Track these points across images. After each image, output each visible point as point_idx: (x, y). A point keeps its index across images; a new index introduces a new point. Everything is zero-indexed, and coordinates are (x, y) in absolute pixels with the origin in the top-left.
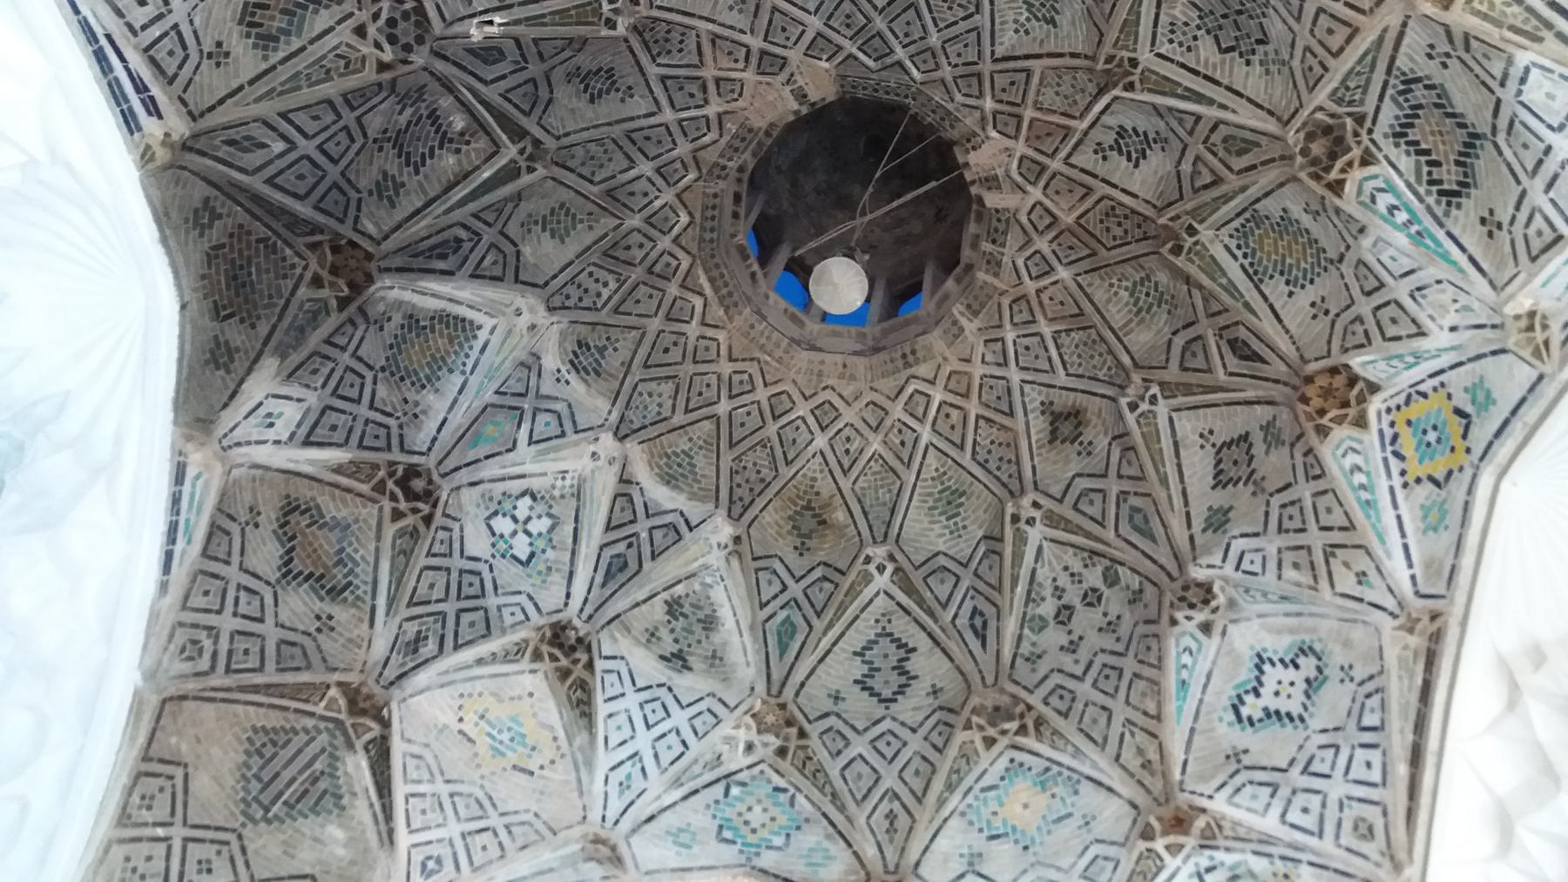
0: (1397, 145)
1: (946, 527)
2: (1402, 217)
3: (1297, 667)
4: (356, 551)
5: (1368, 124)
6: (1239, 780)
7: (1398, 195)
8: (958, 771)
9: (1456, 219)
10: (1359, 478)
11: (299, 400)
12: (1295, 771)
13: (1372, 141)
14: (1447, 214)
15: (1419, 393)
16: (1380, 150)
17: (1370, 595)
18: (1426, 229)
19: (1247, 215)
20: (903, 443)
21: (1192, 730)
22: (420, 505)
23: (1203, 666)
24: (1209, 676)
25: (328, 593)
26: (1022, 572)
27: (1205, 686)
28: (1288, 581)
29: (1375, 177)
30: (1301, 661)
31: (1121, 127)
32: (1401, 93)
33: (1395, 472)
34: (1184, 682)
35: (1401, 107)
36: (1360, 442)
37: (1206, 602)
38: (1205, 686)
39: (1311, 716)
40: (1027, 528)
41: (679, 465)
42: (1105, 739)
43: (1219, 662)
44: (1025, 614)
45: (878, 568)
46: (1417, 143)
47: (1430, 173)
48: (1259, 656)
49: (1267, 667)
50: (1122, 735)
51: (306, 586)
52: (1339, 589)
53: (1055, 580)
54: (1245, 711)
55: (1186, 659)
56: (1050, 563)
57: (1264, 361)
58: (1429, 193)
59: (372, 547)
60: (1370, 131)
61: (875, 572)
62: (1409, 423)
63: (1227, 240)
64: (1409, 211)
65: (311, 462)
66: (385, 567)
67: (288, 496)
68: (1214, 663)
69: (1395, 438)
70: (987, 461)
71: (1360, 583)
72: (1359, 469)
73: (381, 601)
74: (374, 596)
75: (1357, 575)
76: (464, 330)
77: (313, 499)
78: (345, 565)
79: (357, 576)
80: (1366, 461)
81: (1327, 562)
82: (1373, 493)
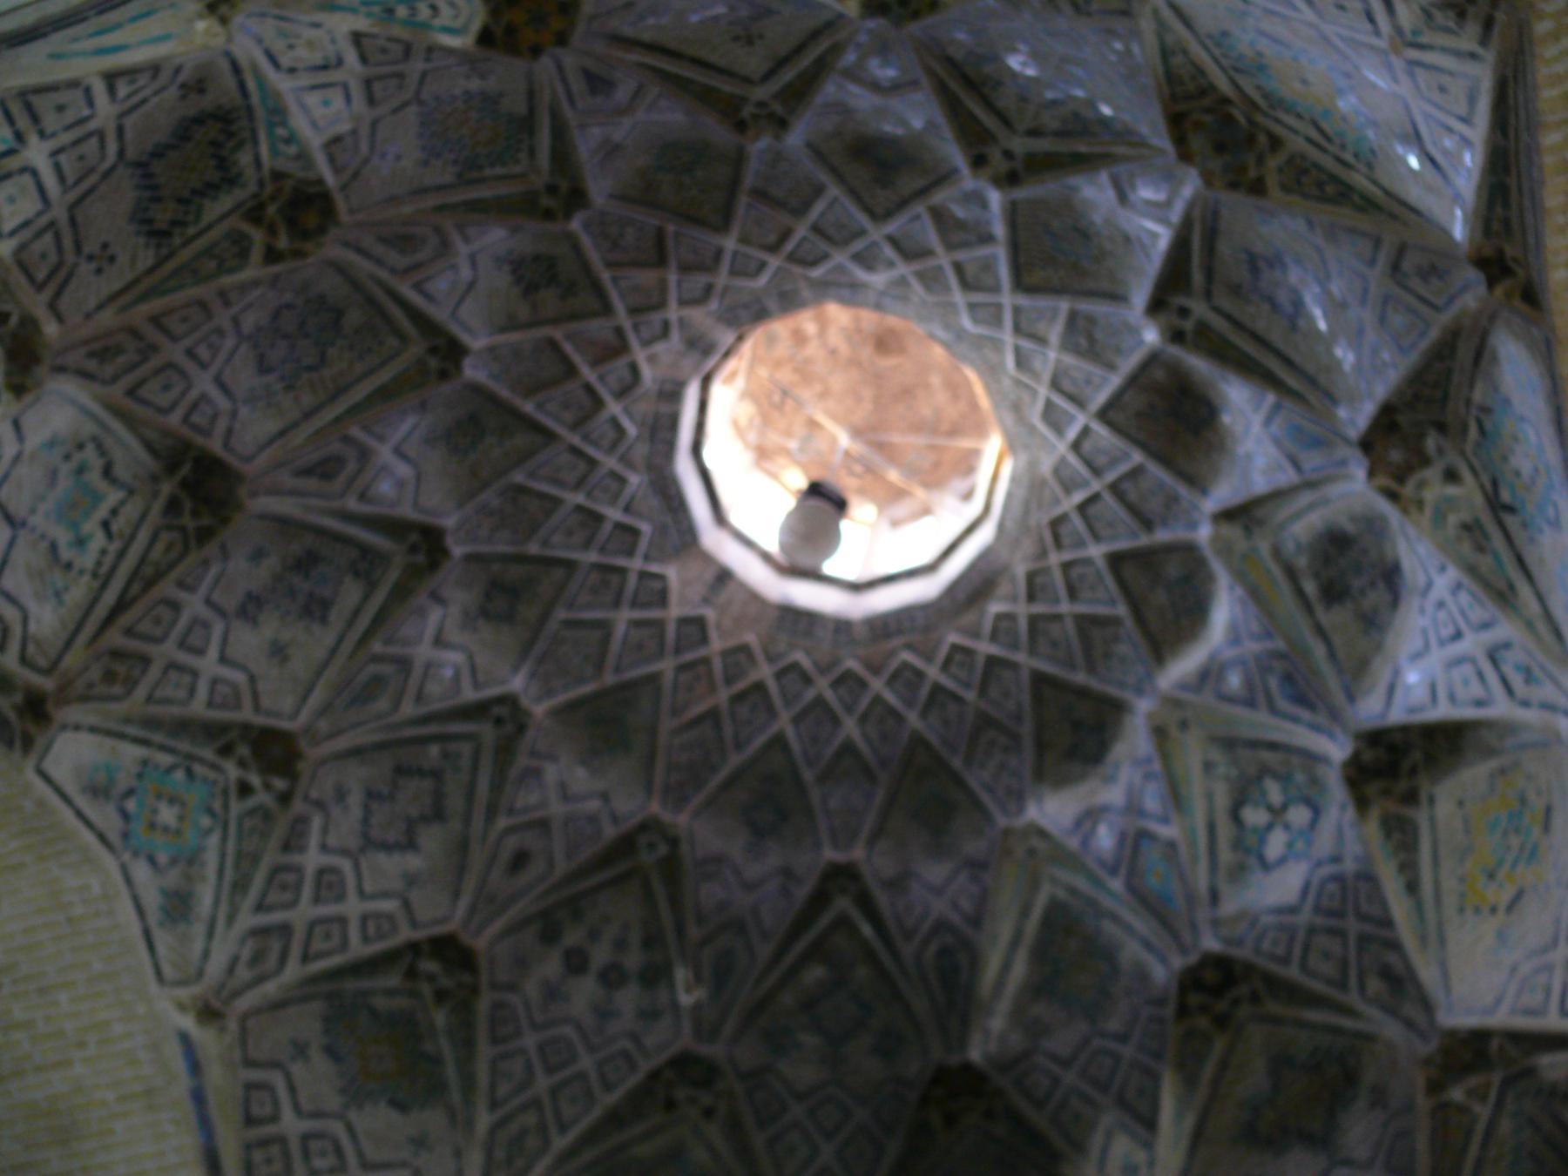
2: (281, 131)
8: (1320, 185)
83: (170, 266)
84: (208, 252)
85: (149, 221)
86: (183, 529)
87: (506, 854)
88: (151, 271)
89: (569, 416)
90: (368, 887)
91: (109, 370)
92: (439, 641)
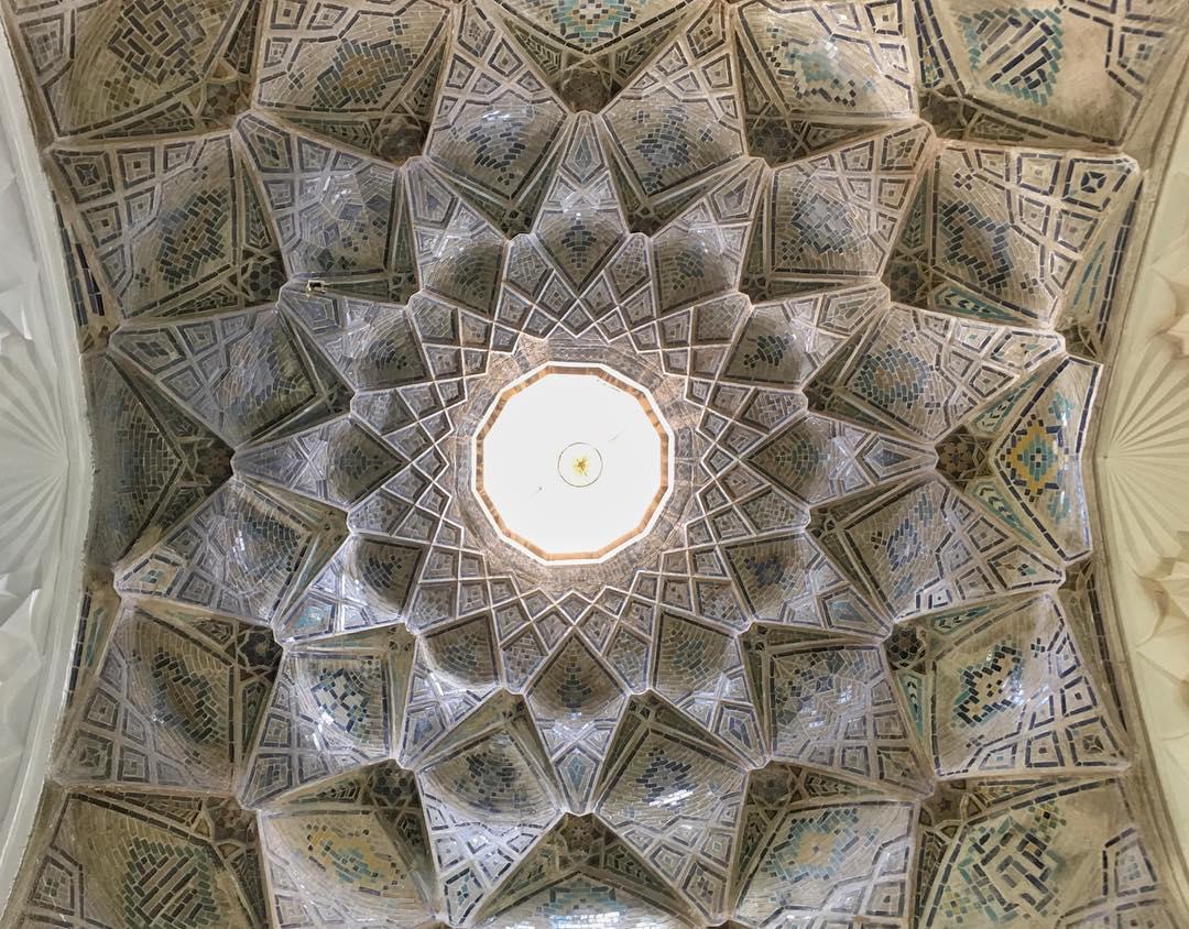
0: (953, 264)
1: (692, 674)
2: (970, 306)
3: (999, 669)
5: (930, 257)
6: (983, 755)
7: (963, 294)
9: (1006, 293)
10: (997, 505)
11: (174, 564)
12: (1025, 729)
14: (999, 293)
15: (1018, 433)
17: (1033, 578)
20: (642, 618)
23: (927, 694)
24: (933, 700)
27: (933, 706)
29: (946, 289)
32: (946, 224)
33: (1022, 495)
35: (949, 235)
36: (990, 483)
37: (914, 650)
38: (933, 706)
39: (1020, 654)
41: (460, 658)
42: (868, 768)
44: (774, 712)
45: (642, 713)
46: (965, 257)
47: (979, 273)
49: (976, 680)
50: (880, 760)
52: (1010, 585)
53: (790, 683)
54: (970, 715)
55: (911, 690)
56: (783, 672)
58: (983, 285)
60: (933, 262)
61: (642, 718)
62: (1020, 457)
63: (854, 389)
65: (182, 615)
66: (238, 714)
71: (1024, 574)
72: (997, 499)
75: (1019, 569)
76: (287, 538)
77: (180, 656)
80: (999, 493)
81: (995, 572)
83: (930, 205)
84: (922, 227)
85: (962, 211)
87: (439, 194)
88: (935, 196)
89: (668, 324)
90: (469, 106)
91: (895, 142)
92: (581, 201)
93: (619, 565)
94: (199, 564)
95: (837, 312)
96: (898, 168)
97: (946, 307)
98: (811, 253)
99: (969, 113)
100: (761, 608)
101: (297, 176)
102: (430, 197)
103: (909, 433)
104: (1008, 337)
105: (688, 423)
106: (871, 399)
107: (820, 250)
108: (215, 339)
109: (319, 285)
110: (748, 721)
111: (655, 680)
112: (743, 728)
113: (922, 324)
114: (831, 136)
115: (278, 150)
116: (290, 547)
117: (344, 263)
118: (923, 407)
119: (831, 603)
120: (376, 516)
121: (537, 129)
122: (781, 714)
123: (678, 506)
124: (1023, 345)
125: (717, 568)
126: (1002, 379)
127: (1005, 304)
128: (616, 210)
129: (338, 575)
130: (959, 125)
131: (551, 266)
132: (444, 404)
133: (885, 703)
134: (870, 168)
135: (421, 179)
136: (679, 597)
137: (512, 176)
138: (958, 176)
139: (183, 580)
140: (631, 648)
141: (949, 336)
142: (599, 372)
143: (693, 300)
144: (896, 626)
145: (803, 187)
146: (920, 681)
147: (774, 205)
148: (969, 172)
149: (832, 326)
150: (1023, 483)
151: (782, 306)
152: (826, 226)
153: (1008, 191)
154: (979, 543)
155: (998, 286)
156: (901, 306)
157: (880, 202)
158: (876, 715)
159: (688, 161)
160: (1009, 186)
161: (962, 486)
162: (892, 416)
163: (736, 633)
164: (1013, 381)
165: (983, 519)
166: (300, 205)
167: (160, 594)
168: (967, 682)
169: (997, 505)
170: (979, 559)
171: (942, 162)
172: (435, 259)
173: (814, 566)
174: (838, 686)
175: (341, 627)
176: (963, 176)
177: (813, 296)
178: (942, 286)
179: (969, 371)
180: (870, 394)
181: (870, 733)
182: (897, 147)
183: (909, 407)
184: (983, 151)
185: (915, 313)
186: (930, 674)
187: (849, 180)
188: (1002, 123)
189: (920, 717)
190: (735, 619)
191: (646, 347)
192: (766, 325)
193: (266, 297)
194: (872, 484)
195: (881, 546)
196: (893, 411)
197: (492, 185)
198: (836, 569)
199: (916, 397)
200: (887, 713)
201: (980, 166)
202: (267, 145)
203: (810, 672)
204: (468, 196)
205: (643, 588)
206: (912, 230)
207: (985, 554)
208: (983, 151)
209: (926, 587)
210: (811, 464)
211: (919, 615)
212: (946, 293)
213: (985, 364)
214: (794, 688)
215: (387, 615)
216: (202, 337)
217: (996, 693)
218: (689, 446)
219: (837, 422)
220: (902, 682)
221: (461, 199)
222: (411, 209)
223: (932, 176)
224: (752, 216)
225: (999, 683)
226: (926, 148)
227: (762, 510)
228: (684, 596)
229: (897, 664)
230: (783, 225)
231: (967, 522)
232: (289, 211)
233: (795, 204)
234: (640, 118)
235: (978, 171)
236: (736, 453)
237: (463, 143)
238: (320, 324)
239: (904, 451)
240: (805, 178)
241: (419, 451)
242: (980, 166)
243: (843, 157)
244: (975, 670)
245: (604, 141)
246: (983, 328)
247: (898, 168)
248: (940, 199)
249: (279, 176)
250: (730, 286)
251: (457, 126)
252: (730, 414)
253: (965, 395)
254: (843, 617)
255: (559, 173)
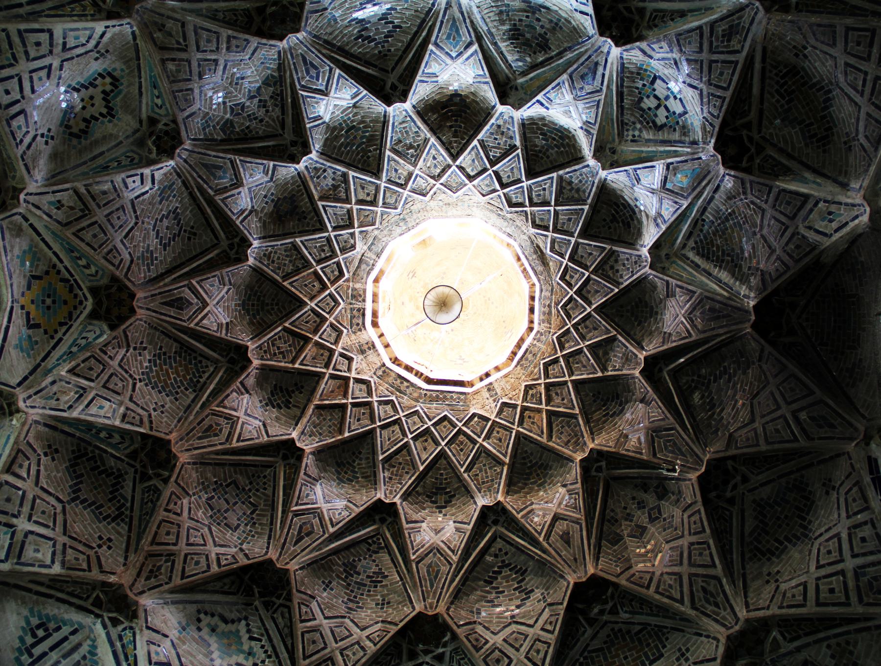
0: (119, 470)
1: (352, 121)
3: (85, 120)
4: (778, 101)
5: (138, 476)
7: (110, 445)
9: (72, 445)
10: (83, 262)
11: (810, 228)
13: (133, 466)
14: (78, 445)
15: (66, 324)
16: (128, 464)
18: (87, 433)
19: (199, 386)
20: (396, 171)
21: (138, 59)
22: (730, 133)
24: (141, 94)
25: (799, 72)
26: (290, 112)
28: (107, 182)
29: (125, 449)
30: (83, 125)
31: (289, 408)
32: (124, 505)
33: (63, 270)
34: (155, 87)
35: (121, 495)
36: (92, 281)
38: (140, 87)
40: (295, 139)
41: (554, 139)
43: (137, 103)
44: (281, 86)
45: (396, 87)
46: (108, 476)
47: (96, 462)
48: (113, 116)
49: (104, 111)
51: (815, 80)
52: (71, 192)
53: (267, 111)
54: (108, 80)
55: (159, 102)
56: (273, 120)
57: (163, 303)
58: (93, 452)
59: (766, 104)
60: (136, 472)
61: (397, 84)
62: (65, 302)
63: (209, 363)
64: (102, 440)
65: (804, 181)
66: (756, 90)
67: (824, 151)
68: (140, 102)
69: (71, 291)
70: (334, 173)
71: (59, 201)
72: (84, 267)
73: (758, 66)
74: (763, 69)
75: (63, 206)
76: (703, 248)
77: (807, 145)
78: (786, 91)
79: (777, 82)
80: (83, 272)
81: (84, 204)
82: (71, 257)
83: (135, 522)
84: (143, 503)
85: (108, 516)
86: (281, 605)
87: (559, 545)
88: (130, 530)
89: (367, 422)
91: (163, 578)
92: (437, 532)
93: (415, 216)
94: (787, 228)
95: (221, 430)
96: (161, 555)
97: (123, 433)
98: (242, 480)
99: (98, 603)
100: (293, 177)
101: (684, 569)
102: (568, 542)
103: (161, 326)
104: (70, 407)
105: (353, 337)
106: (194, 355)
107: (234, 483)
108: (764, 429)
109: (668, 470)
110: (303, 78)
111: (385, 116)
112: (308, 73)
113: (146, 420)
114: (218, 585)
115: (701, 595)
116: (701, 241)
117: (645, 488)
118: (149, 347)
119: (232, 180)
120: (624, 265)
121: (473, 597)
122: (275, 84)
123: (363, 266)
124: (58, 400)
125: (330, 212)
126: (76, 371)
127: (73, 436)
128: (408, 522)
129: (659, 215)
130: (106, 593)
131: (466, 475)
132: (561, 359)
133: (181, 91)
134: (186, 555)
135: (575, 559)
136: (363, 188)
137: (496, 556)
138: (109, 548)
139: (803, 213)
140: (406, 145)
141: (122, 410)
142: (429, 381)
143: (345, 442)
144: (172, 158)
145: (246, 538)
146: (153, 111)
147: (272, 524)
148: (100, 551)
149: (226, 418)
150: (62, 280)
151: (268, 436)
152: (228, 504)
153: (65, 534)
154: (98, 229)
155: (79, 450)
156: (162, 436)
157: (179, 526)
158: (190, 80)
159: (344, 564)
160: (62, 539)
161: (114, 279)
162: (176, 340)
163: (314, 155)
164: (66, 369)
165: (95, 250)
166: (684, 542)
167: (825, 201)
168: (112, 109)
169: (83, 262)
170: (100, 215)
171: (122, 560)
172: (564, 486)
173: (246, 213)
174: (225, 108)
175: (659, 167)
176: (105, 547)
177: (241, 444)
178: (128, 451)
179: (106, 378)
180: (195, 358)
181: (194, 64)
182: (161, 574)
183: (161, 348)
184: (84, 570)
185: (151, 429)
186: (144, 116)
187: (205, 545)
188: (68, 593)
189: (151, 77)
190: (315, 168)
191: (387, 403)
192: (284, 418)
193: (715, 465)
194: (194, 282)
195: (189, 229)
196: (175, 344)
197: (513, 550)
198: (226, 210)
199: (155, 355)
200: (180, 81)
201: (88, 556)
202: (712, 599)
203: (250, 120)
204: (534, 542)
205: (395, 197)
206: (152, 501)
207: (93, 220)
208: (84, 570)
209: (147, 192)
210: (249, 299)
211: (152, 168)
212: (125, 445)
213: (92, 384)
214: (264, 106)
215: (617, 178)
216: (777, 431)
217: (86, 99)
218: (352, 317)
219: (223, 335)
220: (167, 109)
221: (541, 539)
222: (584, 533)
223: (132, 548)
224: (290, 515)
225: (84, 108)
226: (134, 572)
227: (290, 261)
228: (359, 189)
229: (173, 126)
230: (265, 505)
231: (109, 247)
232: (694, 539)
233: (254, 523)
234: (384, 603)
235: (91, 553)
236: (313, 310)
237: (537, 588)
238: (669, 435)
239: (165, 310)
240: (244, 547)
241: (584, 320)
242: (88, 556)
243: (208, 566)
244: (106, 120)
245: (415, 585)
246: (92, 415)
247: (161, 555)
248: (126, 528)
249: (700, 571)
250: (313, 453)
251: (543, 604)
252: (317, 344)
253: (110, 357)
254: (220, 168)
255: (455, 558)
